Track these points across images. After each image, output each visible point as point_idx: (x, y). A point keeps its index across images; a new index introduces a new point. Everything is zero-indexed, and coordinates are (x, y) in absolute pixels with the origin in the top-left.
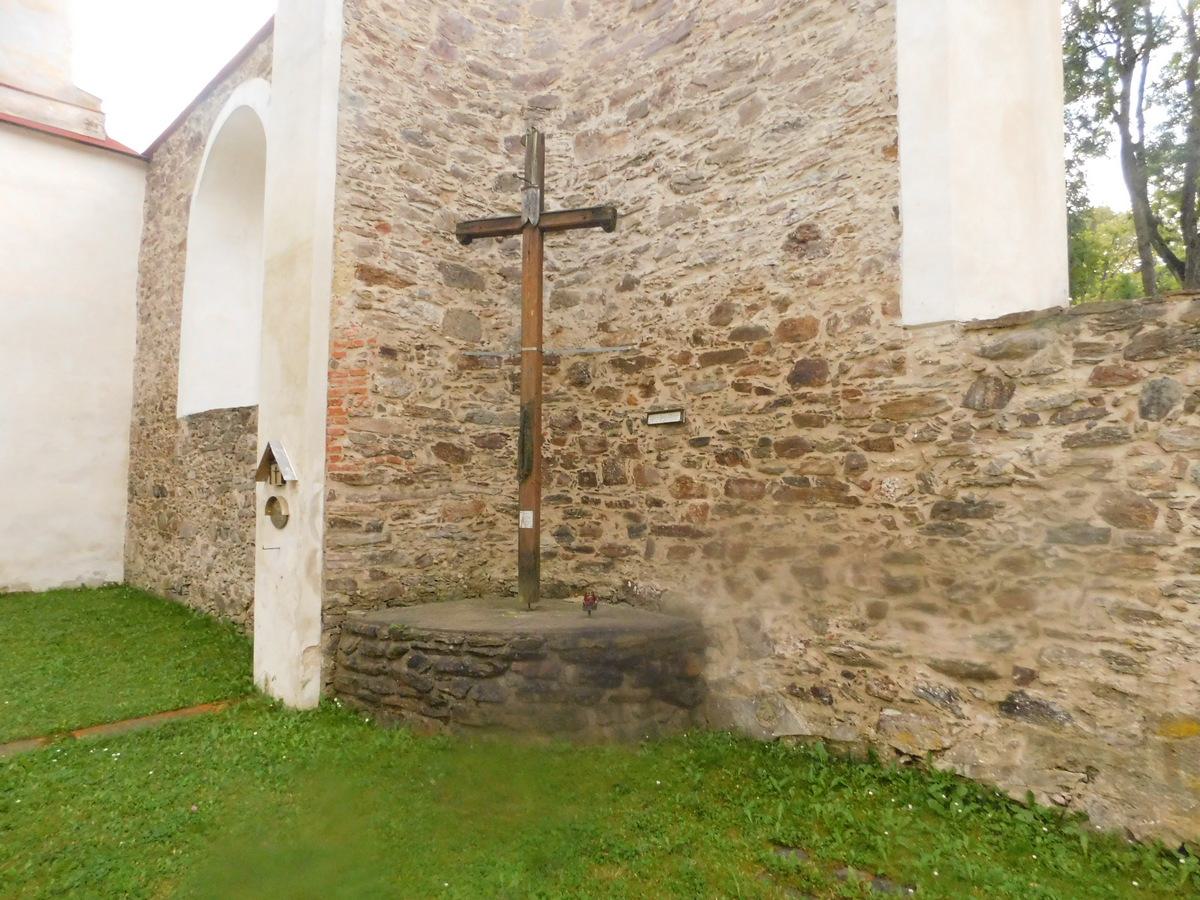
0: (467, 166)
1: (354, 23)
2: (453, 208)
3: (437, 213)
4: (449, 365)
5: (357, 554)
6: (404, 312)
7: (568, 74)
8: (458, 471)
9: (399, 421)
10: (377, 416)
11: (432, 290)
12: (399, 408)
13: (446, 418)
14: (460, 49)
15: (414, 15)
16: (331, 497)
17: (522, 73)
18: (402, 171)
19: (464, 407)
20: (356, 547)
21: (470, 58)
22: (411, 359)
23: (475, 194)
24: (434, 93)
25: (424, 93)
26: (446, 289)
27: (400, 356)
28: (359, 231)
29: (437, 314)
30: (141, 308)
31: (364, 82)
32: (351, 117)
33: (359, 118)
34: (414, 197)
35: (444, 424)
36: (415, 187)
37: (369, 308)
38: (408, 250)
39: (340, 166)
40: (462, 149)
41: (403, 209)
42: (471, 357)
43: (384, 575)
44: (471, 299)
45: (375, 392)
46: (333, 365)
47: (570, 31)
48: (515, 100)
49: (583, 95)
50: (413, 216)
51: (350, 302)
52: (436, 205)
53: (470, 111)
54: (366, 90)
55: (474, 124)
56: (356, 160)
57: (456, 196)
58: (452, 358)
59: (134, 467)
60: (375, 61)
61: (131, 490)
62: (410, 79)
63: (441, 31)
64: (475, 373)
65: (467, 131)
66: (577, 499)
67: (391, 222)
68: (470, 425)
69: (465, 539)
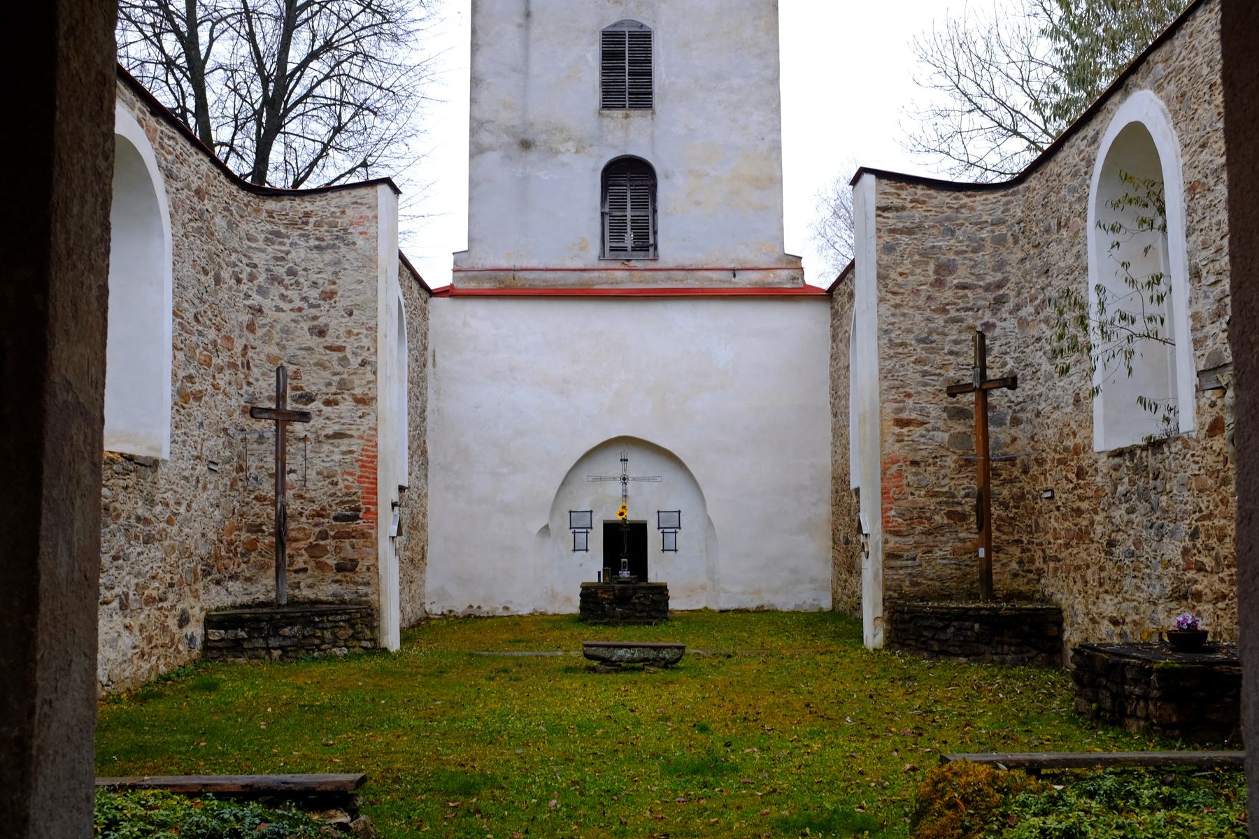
0: (959, 346)
1: (884, 290)
2: (951, 374)
3: (941, 379)
4: (953, 466)
5: (901, 572)
6: (922, 440)
7: (1013, 279)
8: (962, 526)
9: (924, 500)
10: (910, 498)
11: (940, 424)
12: (923, 493)
13: (953, 496)
14: (949, 279)
15: (918, 271)
16: (886, 542)
17: (988, 281)
18: (917, 362)
19: (964, 489)
20: (901, 568)
21: (955, 282)
22: (929, 465)
23: (965, 362)
24: (934, 311)
25: (928, 313)
26: (949, 423)
27: (922, 464)
28: (895, 401)
29: (944, 437)
30: (833, 405)
31: (892, 320)
32: (886, 341)
33: (890, 340)
34: (925, 374)
35: (951, 500)
36: (925, 368)
37: (903, 441)
38: (924, 405)
39: (881, 370)
40: (954, 337)
41: (919, 382)
42: (966, 460)
43: (918, 584)
44: (965, 424)
45: (908, 485)
46: (883, 474)
47: (1011, 253)
48: (985, 299)
49: (1019, 294)
50: (926, 385)
51: (891, 439)
52: (940, 374)
53: (958, 314)
54: (893, 324)
55: (961, 320)
56: (889, 364)
57: (953, 366)
58: (955, 462)
60: (897, 306)
61: (833, 539)
62: (919, 308)
63: (936, 272)
64: (969, 469)
65: (956, 326)
66: (1025, 542)
67: (912, 391)
68: (968, 499)
69: (967, 565)
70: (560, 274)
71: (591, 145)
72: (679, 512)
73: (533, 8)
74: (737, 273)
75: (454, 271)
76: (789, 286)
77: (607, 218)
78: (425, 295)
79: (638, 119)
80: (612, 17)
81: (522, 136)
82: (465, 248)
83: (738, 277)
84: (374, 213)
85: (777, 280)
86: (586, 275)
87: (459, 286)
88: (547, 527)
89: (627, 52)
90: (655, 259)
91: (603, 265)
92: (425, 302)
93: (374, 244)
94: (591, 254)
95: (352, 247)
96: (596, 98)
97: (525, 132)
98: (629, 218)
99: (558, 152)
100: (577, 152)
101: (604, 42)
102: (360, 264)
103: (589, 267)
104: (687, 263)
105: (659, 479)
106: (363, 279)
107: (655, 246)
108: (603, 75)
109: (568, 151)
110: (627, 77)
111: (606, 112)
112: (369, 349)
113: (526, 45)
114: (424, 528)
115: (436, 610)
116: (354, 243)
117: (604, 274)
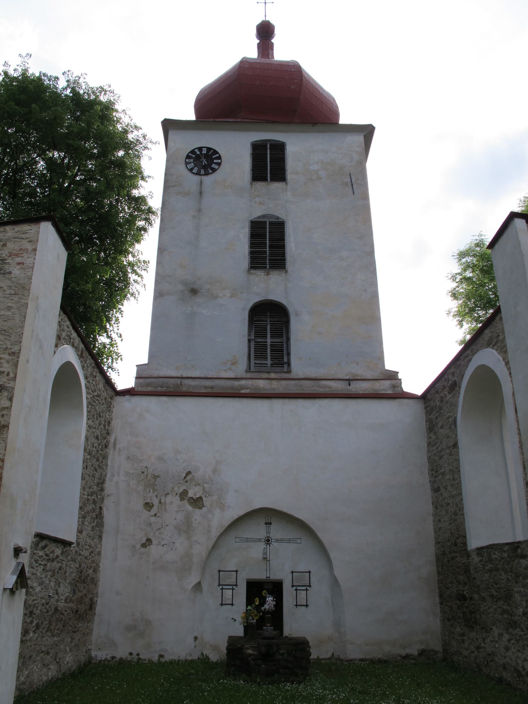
30: (433, 483)
59: (440, 582)
61: (441, 596)
70: (217, 382)
71: (241, 293)
72: (310, 572)
74: (351, 382)
75: (137, 378)
77: (253, 344)
78: (111, 392)
79: (275, 277)
80: (257, 213)
82: (146, 362)
83: (352, 386)
84: (34, 247)
85: (381, 388)
86: (237, 383)
87: (140, 389)
88: (199, 584)
89: (268, 234)
90: (289, 372)
91: (249, 375)
92: (111, 398)
93: (29, 274)
94: (241, 368)
95: (7, 276)
96: (245, 262)
98: (269, 343)
99: (216, 297)
100: (232, 296)
102: (13, 292)
103: (239, 377)
104: (313, 376)
105: (299, 541)
106: (14, 305)
107: (289, 364)
108: (251, 247)
109: (224, 296)
110: (268, 249)
111: (253, 271)
112: (8, 374)
114: (94, 582)
115: (100, 655)
116: (10, 273)
117: (250, 382)
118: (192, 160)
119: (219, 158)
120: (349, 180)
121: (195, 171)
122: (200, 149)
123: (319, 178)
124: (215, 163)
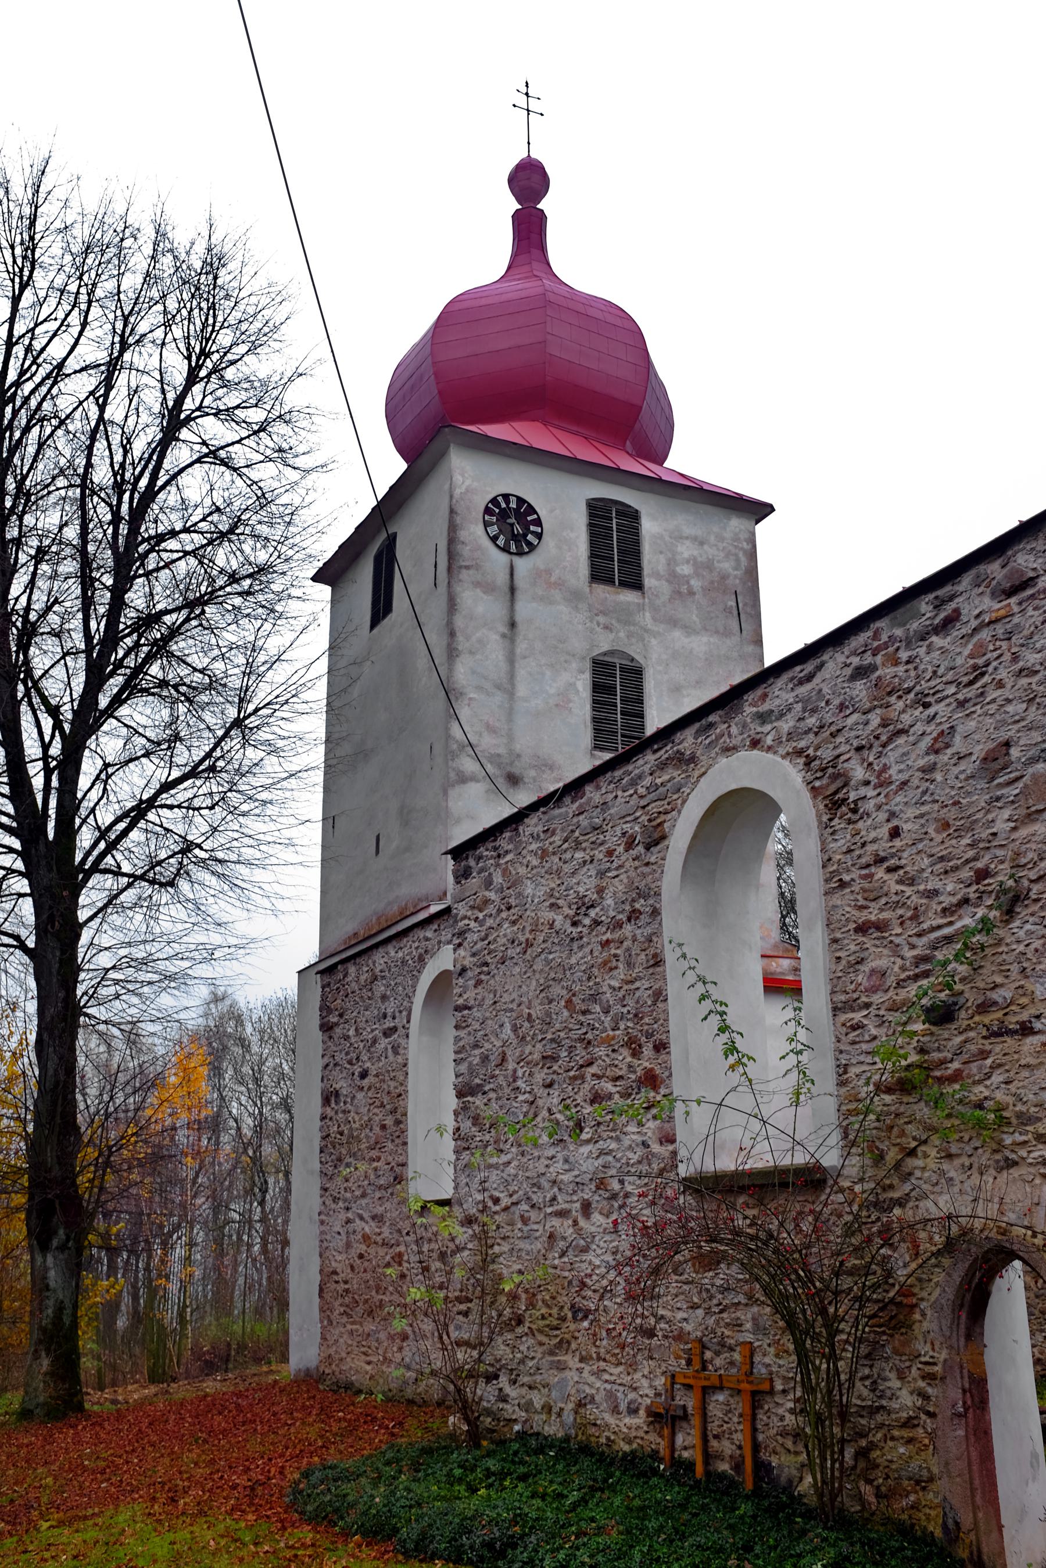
73: (519, 618)
76: (791, 978)
80: (604, 644)
81: (509, 769)
85: (779, 970)
97: (512, 763)
101: (595, 672)
113: (511, 660)
118: (494, 519)
119: (538, 522)
120: (734, 604)
121: (501, 541)
122: (506, 497)
123: (691, 593)
124: (533, 533)
